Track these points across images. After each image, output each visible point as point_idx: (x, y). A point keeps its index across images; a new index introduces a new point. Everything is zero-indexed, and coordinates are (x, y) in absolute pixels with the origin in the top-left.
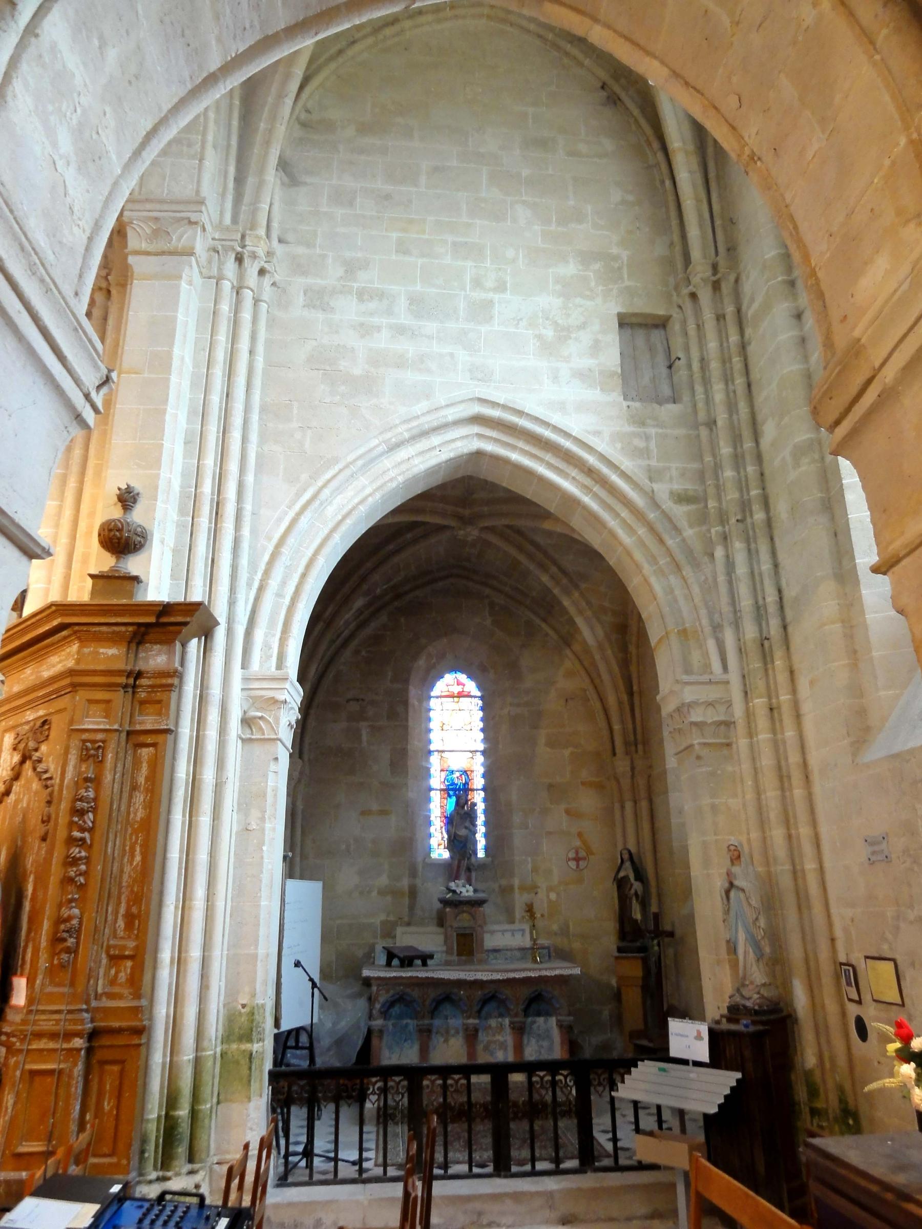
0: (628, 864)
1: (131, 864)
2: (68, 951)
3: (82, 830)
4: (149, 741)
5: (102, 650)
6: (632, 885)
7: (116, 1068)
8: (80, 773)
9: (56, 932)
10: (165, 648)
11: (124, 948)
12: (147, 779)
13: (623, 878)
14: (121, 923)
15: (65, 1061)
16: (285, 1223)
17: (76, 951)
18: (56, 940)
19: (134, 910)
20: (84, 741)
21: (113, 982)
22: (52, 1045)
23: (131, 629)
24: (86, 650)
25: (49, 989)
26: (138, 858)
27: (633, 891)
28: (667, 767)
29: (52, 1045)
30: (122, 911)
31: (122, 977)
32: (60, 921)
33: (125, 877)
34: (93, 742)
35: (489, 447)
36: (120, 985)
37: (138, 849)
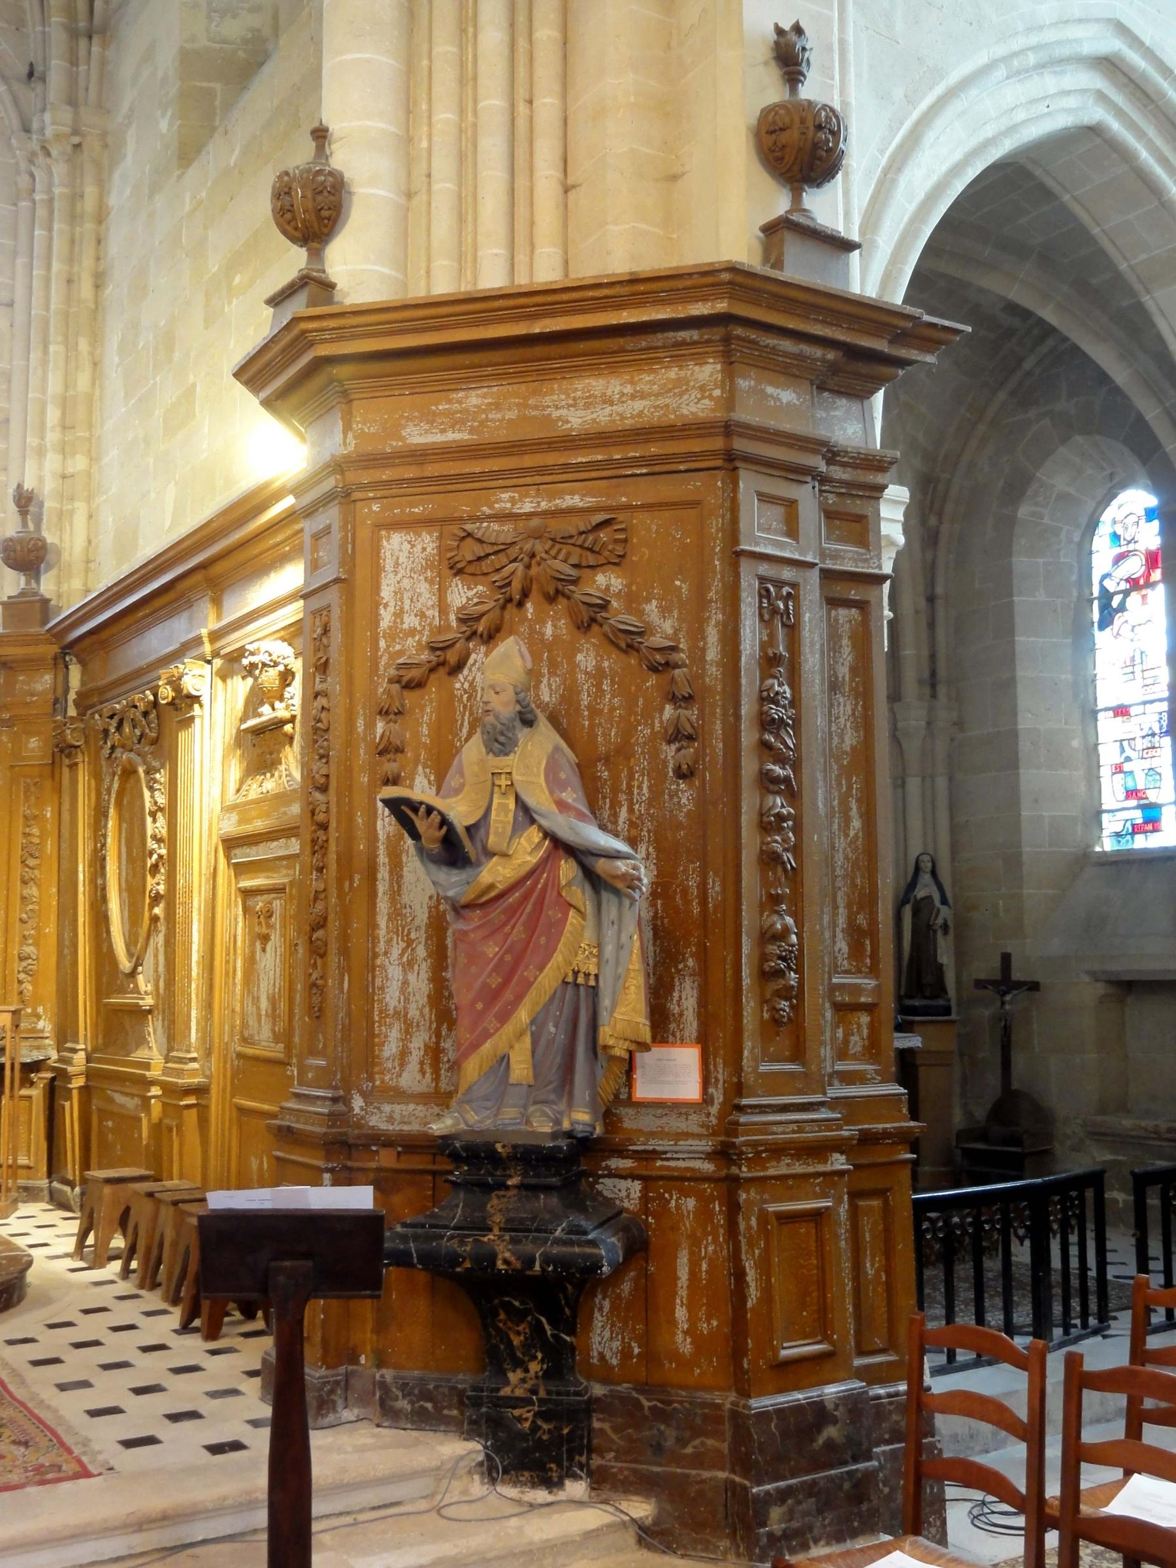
0: (926, 878)
1: (846, 835)
2: (785, 993)
3: (781, 760)
4: (853, 595)
5: (770, 390)
6: (939, 910)
7: (876, 1203)
8: (763, 646)
9: (764, 958)
10: (855, 407)
11: (856, 989)
12: (853, 670)
13: (922, 899)
14: (842, 945)
15: (824, 1195)
16: (957, 1435)
17: (800, 995)
18: (766, 975)
19: (862, 920)
20: (762, 579)
21: (842, 1054)
22: (799, 1168)
23: (831, 356)
24: (743, 384)
25: (764, 1068)
26: (856, 824)
27: (940, 921)
28: (1020, 727)
29: (799, 1168)
30: (842, 921)
31: (857, 1043)
32: (768, 937)
33: (839, 858)
34: (779, 584)
35: (1115, 126)
36: (855, 1057)
37: (854, 805)
